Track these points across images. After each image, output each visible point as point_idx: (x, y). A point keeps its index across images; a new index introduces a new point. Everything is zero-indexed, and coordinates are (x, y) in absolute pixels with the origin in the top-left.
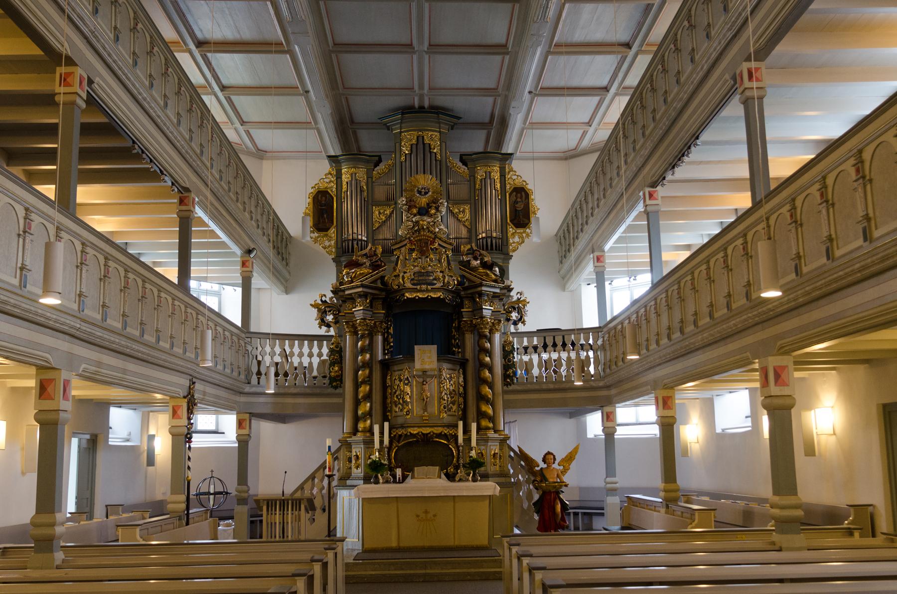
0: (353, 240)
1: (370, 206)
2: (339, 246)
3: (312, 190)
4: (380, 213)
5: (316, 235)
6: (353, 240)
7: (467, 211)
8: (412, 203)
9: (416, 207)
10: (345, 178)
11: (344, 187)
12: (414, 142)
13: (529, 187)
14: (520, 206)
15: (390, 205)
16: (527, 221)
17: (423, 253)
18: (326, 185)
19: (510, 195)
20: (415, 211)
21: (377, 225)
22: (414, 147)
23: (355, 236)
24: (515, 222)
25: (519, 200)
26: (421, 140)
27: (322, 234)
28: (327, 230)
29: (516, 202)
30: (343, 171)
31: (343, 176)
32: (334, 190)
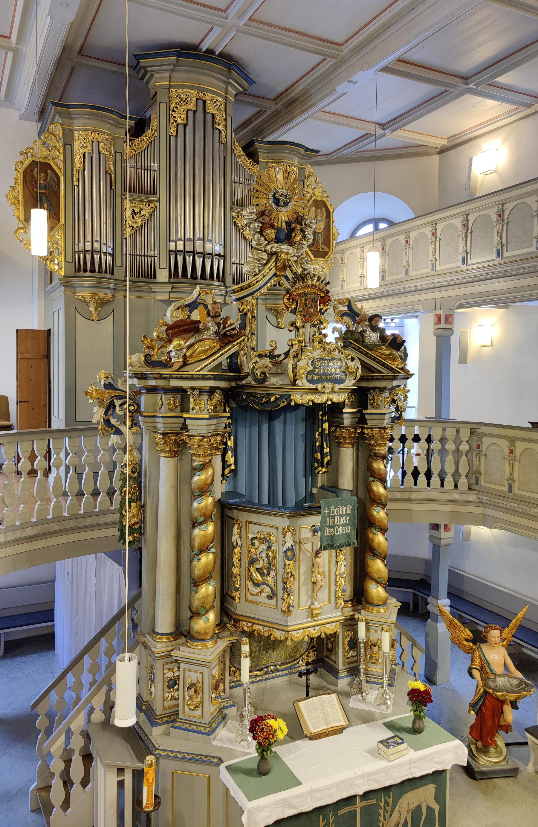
0: (93, 252)
1: (118, 200)
2: (69, 259)
3: (22, 158)
4: (134, 212)
6: (93, 252)
8: (267, 219)
9: (273, 226)
10: (80, 147)
11: (78, 161)
12: (191, 106)
15: (148, 203)
16: (326, 250)
17: (307, 318)
18: (46, 153)
20: (271, 233)
22: (191, 114)
23: (97, 246)
24: (313, 248)
26: (201, 103)
30: (76, 134)
31: (77, 144)
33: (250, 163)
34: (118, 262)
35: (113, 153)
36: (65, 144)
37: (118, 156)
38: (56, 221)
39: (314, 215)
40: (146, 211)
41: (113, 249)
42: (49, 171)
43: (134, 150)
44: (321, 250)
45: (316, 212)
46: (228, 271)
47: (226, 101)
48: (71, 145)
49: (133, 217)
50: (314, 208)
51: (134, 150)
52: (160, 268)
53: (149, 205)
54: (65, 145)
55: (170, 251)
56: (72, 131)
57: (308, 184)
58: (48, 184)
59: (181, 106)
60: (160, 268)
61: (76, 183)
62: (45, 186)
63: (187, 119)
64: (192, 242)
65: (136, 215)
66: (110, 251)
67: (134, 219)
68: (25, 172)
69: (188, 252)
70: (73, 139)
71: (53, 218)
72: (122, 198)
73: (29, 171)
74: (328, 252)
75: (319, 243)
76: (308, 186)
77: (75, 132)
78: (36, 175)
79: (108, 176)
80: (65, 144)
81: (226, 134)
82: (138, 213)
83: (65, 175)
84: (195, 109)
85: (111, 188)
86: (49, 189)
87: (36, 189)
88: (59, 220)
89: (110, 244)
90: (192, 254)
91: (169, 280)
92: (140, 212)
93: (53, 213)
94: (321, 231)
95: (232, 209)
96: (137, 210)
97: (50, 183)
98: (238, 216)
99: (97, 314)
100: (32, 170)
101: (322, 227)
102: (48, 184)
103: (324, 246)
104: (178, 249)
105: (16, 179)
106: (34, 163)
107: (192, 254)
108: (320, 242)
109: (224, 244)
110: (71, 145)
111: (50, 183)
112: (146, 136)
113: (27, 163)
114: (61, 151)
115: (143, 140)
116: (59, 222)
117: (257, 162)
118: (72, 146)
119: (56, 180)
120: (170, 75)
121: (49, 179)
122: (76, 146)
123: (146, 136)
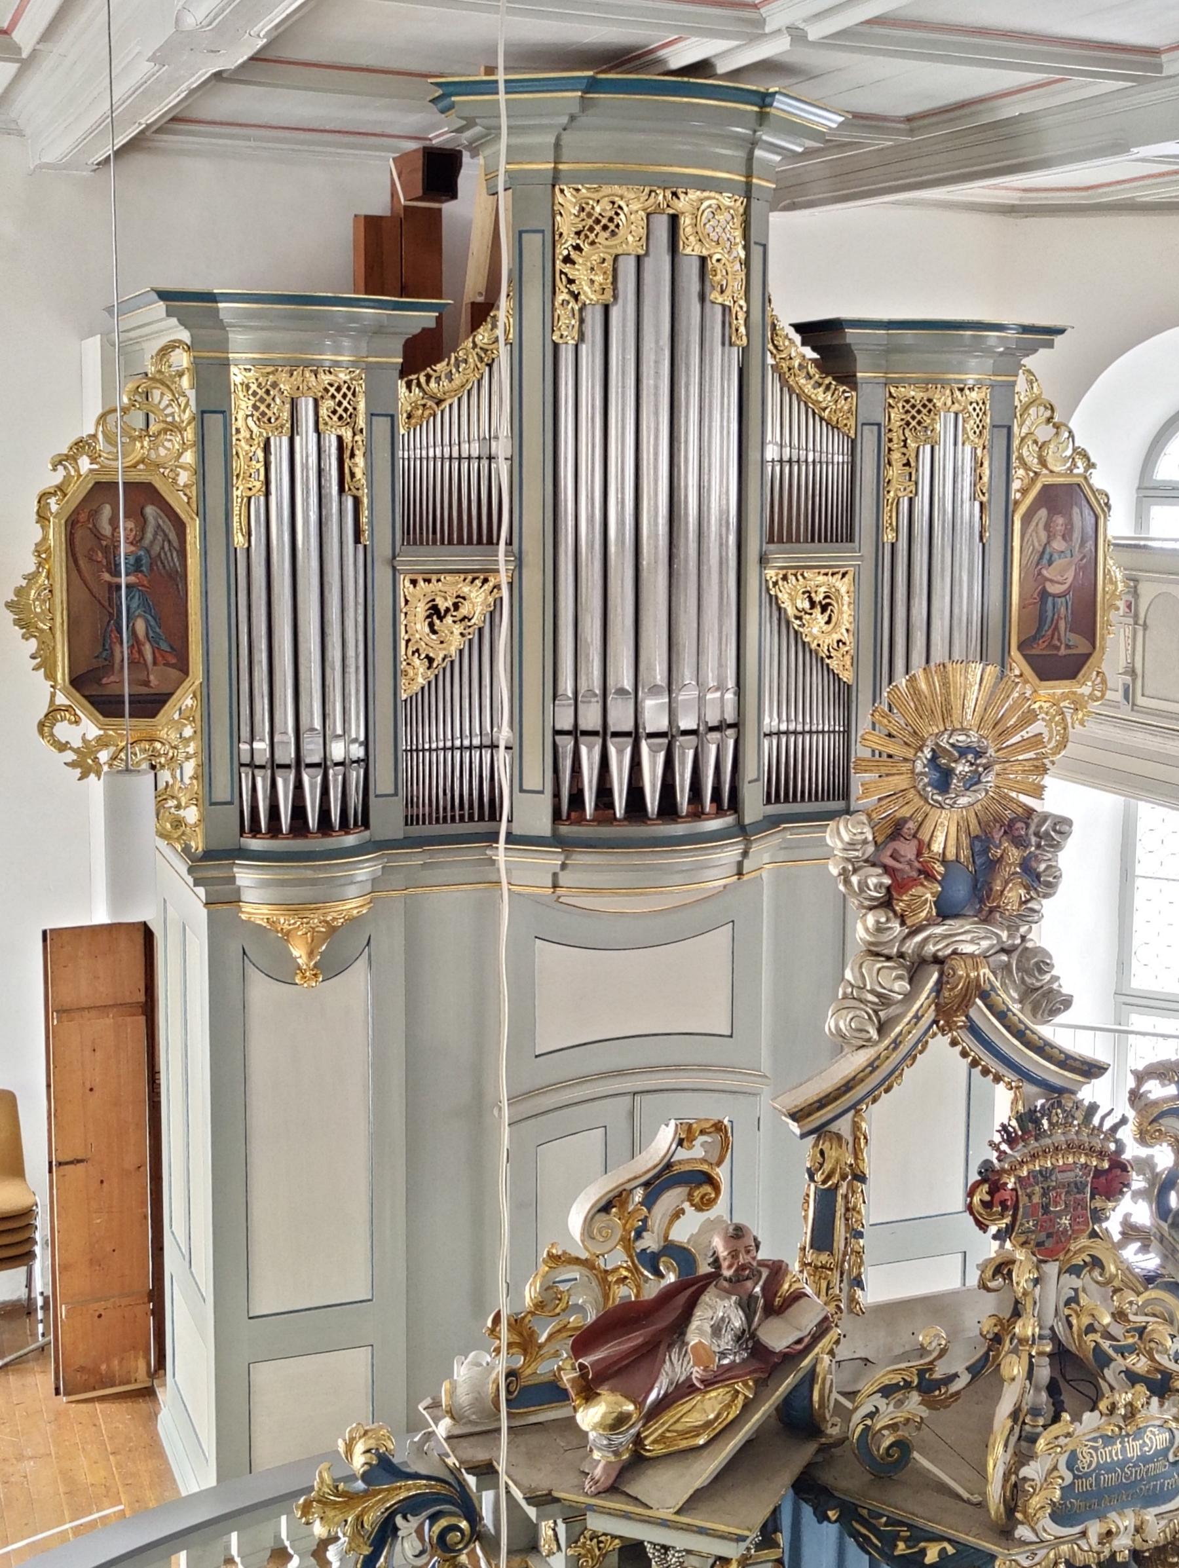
1: (382, 575)
4: (435, 612)
5: (89, 728)
7: (845, 613)
13: (1098, 480)
14: (1061, 577)
16: (1082, 647)
19: (1027, 519)
21: (420, 675)
25: (1058, 545)
27: (128, 726)
28: (149, 705)
29: (1044, 557)
30: (237, 376)
31: (242, 406)
32: (184, 478)
33: (828, 388)
34: (383, 782)
35: (361, 423)
36: (203, 412)
37: (382, 424)
38: (174, 673)
39: (1043, 535)
40: (477, 600)
41: (366, 744)
42: (150, 510)
43: (432, 397)
44: (1063, 651)
45: (1047, 527)
46: (750, 770)
47: (748, 197)
48: (223, 412)
49: (431, 625)
50: (1043, 513)
51: (432, 397)
52: (522, 790)
53: (485, 581)
54: (202, 413)
55: (557, 732)
56: (225, 364)
57: (1023, 435)
58: (148, 551)
59: (593, 243)
60: (522, 790)
61: (239, 540)
62: (138, 560)
63: (615, 289)
64: (632, 701)
65: (441, 618)
66: (358, 752)
67: (434, 632)
68: (72, 524)
69: (615, 734)
70: (225, 389)
71: (167, 664)
72: (394, 569)
73: (83, 517)
74: (1088, 656)
75: (1056, 628)
76: (1023, 439)
77: (233, 369)
78: (106, 530)
79: (349, 503)
80: (203, 412)
81: (748, 312)
82: (447, 610)
83: (202, 513)
84: (642, 252)
85: (357, 540)
86: (151, 570)
87: (107, 576)
88: (184, 669)
89: (357, 730)
90: (630, 740)
91: (554, 831)
92: (456, 606)
93: (164, 646)
94: (1066, 586)
95: (763, 561)
96: (443, 605)
97: (157, 548)
98: (785, 578)
99: (316, 966)
100: (95, 514)
101: (1070, 575)
102: (148, 551)
103: (1074, 639)
104: (584, 725)
105: (41, 550)
106: (102, 489)
107: (630, 740)
108: (1062, 624)
109: (738, 684)
110: (223, 412)
111: (157, 548)
112: (475, 345)
113: (77, 492)
114: (189, 435)
115: (466, 361)
116: (187, 674)
117: (847, 378)
118: (225, 413)
119: (172, 536)
120: (558, 139)
121: (149, 536)
122: (240, 416)
123: (475, 345)
